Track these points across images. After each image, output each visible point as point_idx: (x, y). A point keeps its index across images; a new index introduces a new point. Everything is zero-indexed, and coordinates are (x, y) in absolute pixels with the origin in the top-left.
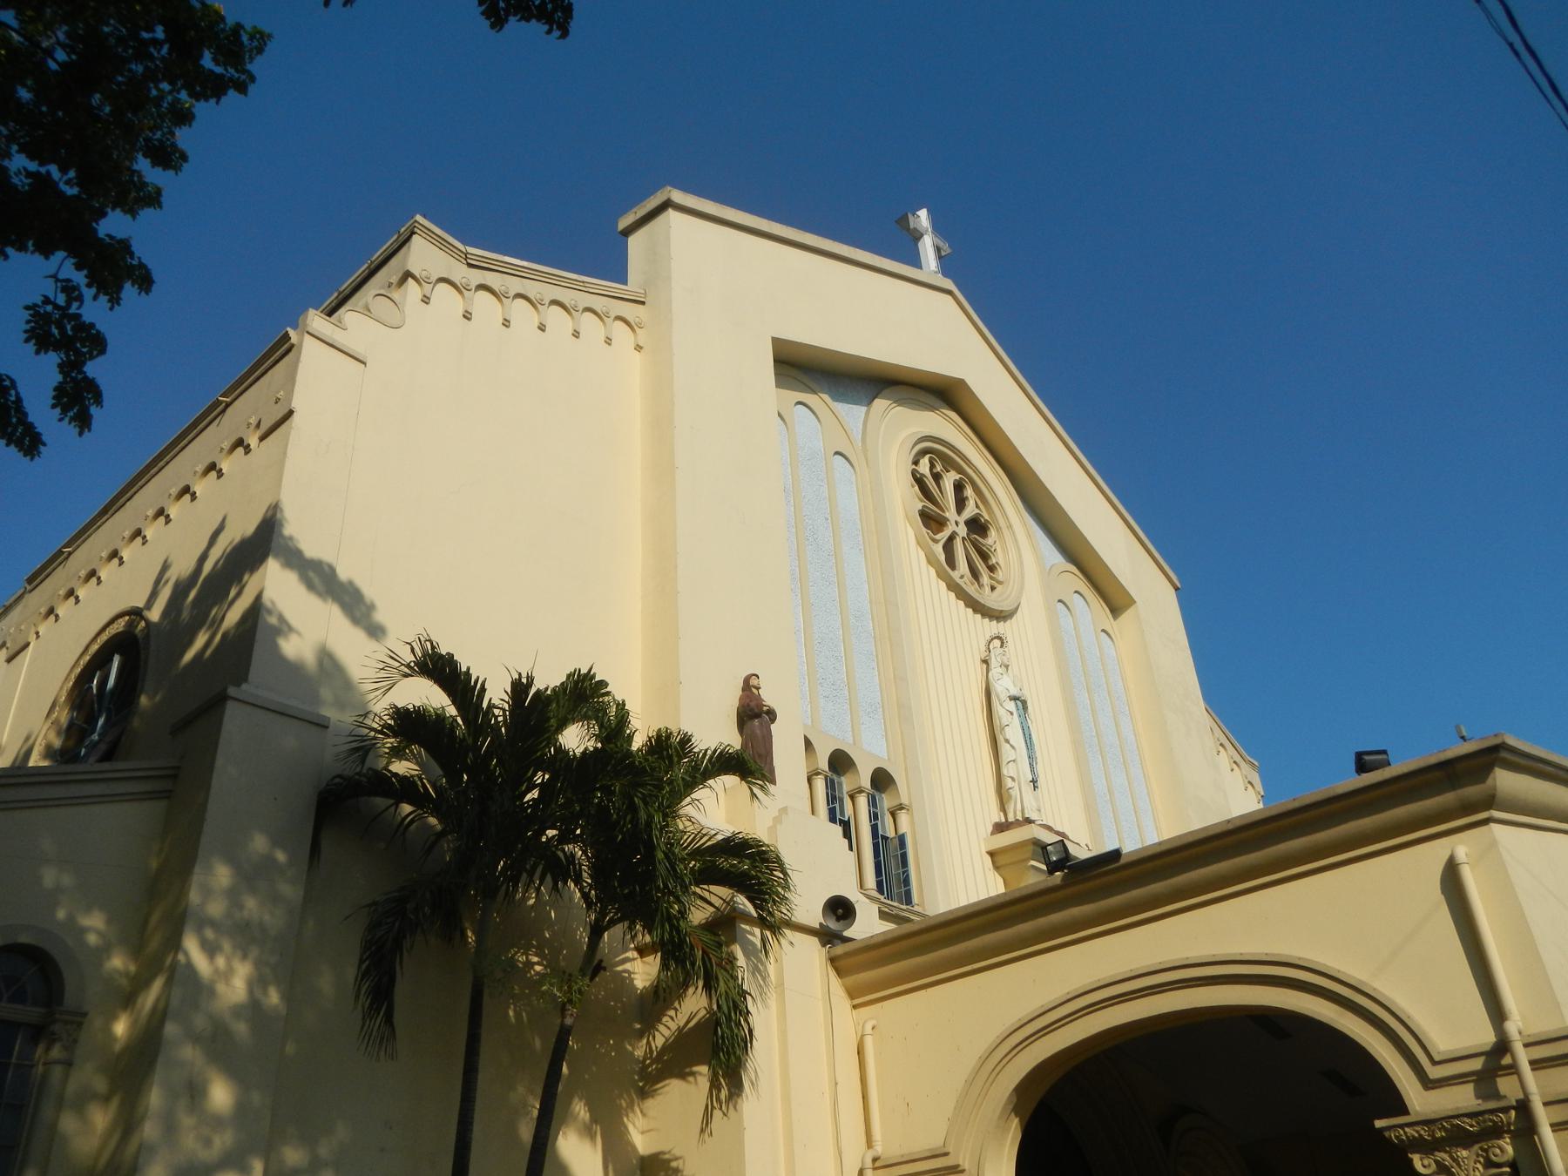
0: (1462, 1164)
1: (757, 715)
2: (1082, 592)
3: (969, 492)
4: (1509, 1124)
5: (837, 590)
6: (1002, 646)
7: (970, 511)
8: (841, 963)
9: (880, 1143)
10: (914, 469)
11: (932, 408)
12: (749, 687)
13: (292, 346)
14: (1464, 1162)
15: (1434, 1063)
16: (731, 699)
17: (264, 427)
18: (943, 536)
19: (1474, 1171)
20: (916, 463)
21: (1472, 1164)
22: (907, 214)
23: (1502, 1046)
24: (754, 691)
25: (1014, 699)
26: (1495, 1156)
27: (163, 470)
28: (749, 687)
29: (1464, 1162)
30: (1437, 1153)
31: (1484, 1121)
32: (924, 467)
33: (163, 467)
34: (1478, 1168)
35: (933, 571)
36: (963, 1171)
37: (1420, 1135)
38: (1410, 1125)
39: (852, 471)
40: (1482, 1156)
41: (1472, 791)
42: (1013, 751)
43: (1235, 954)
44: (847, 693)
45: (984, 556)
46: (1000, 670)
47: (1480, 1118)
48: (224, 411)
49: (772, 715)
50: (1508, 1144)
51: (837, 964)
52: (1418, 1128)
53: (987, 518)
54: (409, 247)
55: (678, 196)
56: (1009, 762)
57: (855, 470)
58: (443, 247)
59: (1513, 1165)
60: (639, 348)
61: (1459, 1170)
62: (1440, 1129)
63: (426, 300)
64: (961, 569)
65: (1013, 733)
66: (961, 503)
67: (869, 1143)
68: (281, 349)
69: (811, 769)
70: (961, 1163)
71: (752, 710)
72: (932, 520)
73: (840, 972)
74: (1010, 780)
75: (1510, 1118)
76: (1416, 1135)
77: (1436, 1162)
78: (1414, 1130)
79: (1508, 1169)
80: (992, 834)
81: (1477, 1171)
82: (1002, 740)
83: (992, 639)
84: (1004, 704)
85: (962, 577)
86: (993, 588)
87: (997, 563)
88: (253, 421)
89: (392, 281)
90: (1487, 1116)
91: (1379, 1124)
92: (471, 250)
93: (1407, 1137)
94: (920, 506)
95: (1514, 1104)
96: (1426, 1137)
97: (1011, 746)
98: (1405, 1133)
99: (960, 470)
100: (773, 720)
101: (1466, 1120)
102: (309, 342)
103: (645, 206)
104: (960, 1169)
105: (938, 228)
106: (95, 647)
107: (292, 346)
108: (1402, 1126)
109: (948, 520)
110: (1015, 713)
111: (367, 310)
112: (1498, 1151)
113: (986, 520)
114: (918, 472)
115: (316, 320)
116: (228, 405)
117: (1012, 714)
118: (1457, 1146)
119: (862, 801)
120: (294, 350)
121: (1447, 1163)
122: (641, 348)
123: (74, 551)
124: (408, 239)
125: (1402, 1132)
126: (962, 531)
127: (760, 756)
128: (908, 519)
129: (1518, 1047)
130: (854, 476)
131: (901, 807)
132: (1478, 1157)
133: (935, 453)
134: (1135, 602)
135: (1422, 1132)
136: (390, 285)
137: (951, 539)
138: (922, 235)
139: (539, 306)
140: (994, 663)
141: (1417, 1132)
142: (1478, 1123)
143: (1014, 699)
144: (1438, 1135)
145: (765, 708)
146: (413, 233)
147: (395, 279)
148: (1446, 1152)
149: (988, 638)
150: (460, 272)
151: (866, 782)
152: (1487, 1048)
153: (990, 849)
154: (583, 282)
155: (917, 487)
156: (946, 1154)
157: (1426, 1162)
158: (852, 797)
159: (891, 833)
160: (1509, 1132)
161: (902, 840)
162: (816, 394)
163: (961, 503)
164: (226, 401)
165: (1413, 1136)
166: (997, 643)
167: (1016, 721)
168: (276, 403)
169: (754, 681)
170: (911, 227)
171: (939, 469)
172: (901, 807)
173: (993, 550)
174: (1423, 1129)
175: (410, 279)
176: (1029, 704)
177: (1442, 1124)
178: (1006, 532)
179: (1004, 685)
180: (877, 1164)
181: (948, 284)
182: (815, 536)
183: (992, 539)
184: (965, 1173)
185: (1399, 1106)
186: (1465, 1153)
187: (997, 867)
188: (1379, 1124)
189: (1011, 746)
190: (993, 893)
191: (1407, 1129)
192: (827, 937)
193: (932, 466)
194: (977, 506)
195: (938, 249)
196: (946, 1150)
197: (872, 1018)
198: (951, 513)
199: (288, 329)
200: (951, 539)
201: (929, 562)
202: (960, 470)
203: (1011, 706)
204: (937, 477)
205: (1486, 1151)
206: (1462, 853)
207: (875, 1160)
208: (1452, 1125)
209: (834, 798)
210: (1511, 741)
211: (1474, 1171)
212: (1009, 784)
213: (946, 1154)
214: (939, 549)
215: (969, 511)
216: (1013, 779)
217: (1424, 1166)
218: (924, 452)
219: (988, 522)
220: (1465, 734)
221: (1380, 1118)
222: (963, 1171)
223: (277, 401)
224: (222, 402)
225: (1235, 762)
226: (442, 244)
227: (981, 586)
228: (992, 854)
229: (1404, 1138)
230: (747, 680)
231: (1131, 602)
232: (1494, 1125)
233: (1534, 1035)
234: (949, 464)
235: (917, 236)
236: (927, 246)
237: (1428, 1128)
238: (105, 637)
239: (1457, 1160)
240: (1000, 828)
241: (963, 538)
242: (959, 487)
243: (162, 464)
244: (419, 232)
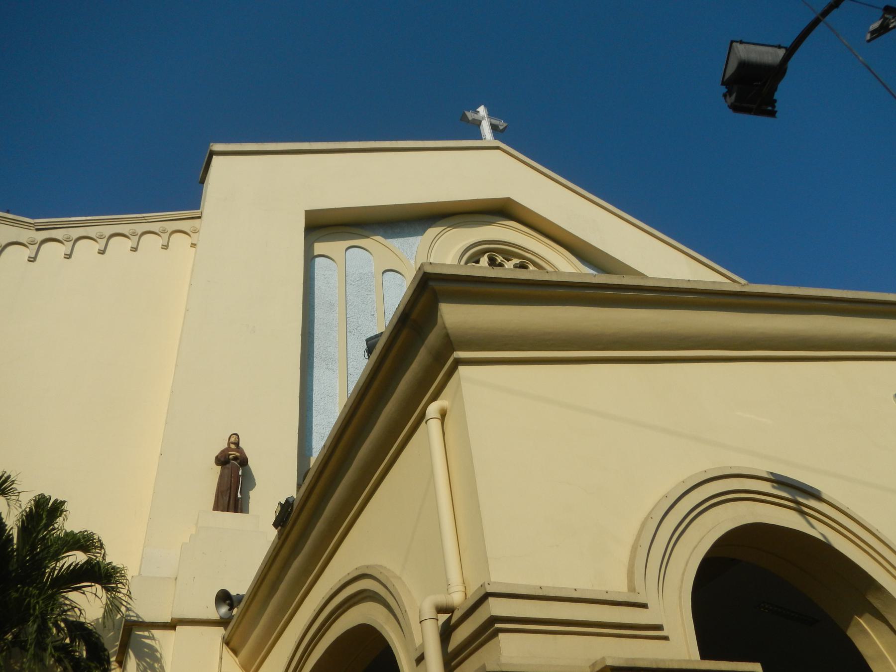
11: (490, 223)
22: (464, 113)
41: (433, 338)
51: (231, 644)
58: (15, 225)
60: (193, 245)
105: (491, 114)
122: (195, 245)
138: (481, 122)
139: (98, 240)
150: (25, 235)
154: (144, 217)
162: (369, 238)
170: (470, 119)
171: (499, 261)
182: (358, 328)
226: (14, 223)
234: (508, 255)
235: (478, 124)
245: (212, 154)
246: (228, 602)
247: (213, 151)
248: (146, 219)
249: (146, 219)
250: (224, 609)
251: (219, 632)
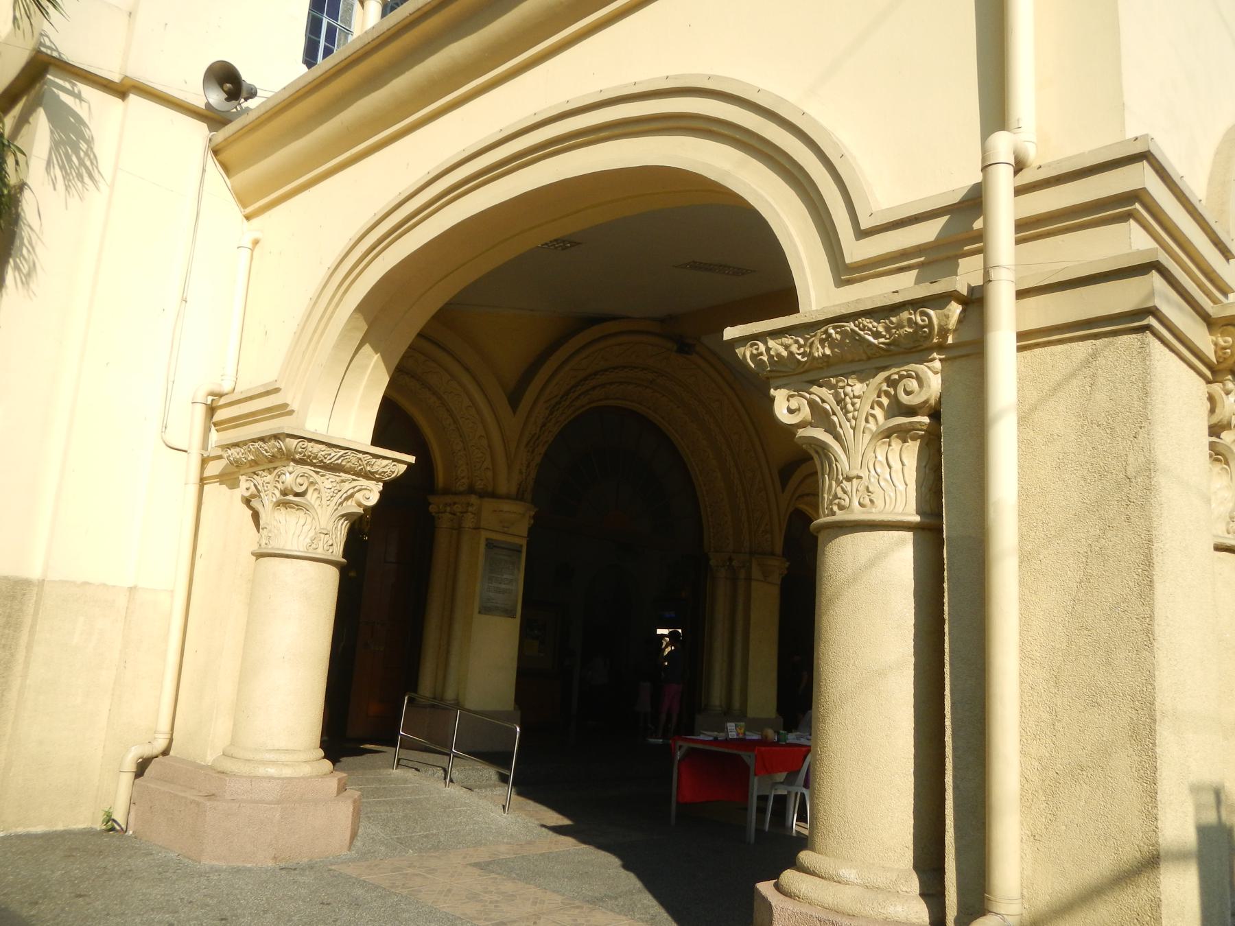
0: (850, 407)
4: (944, 332)
8: (228, 155)
14: (853, 404)
15: (862, 234)
19: (867, 421)
21: (867, 408)
26: (908, 393)
30: (815, 389)
31: (899, 326)
34: (874, 416)
36: (292, 412)
37: (791, 354)
40: (887, 394)
43: (626, 86)
47: (894, 319)
50: (936, 373)
51: (223, 156)
52: (788, 340)
59: (935, 415)
61: (843, 419)
62: (822, 342)
73: (227, 169)
75: (947, 317)
76: (785, 353)
77: (812, 404)
78: (782, 345)
79: (926, 420)
81: (871, 419)
90: (905, 315)
91: (730, 333)
93: (770, 357)
95: (964, 292)
96: (799, 357)
98: (768, 349)
101: (866, 322)
108: (761, 337)
112: (913, 384)
118: (846, 375)
121: (828, 407)
132: (879, 396)
135: (794, 348)
141: (787, 347)
142: (888, 329)
144: (819, 351)
148: (830, 387)
152: (956, 199)
156: (277, 390)
157: (794, 404)
160: (941, 348)
165: (779, 355)
174: (797, 342)
177: (826, 332)
184: (294, 414)
186: (858, 388)
191: (771, 343)
192: (213, 119)
196: (277, 386)
205: (892, 383)
208: (844, 334)
211: (867, 421)
213: (277, 390)
222: (292, 412)
229: (765, 358)
232: (915, 332)
233: (1049, 165)
237: (806, 340)
239: (844, 400)
246: (229, 85)
250: (216, 98)
251: (200, 130)
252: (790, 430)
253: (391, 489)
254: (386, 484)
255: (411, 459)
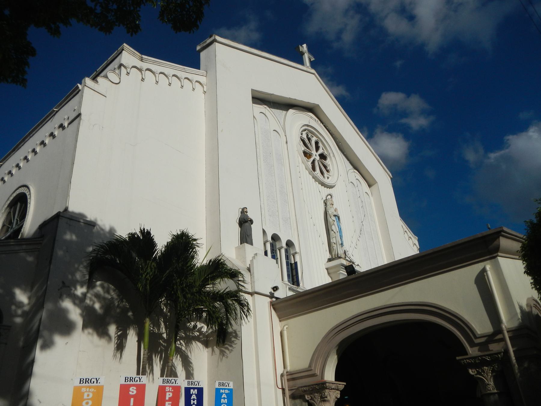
1: (246, 222)
2: (359, 179)
3: (320, 145)
5: (274, 178)
6: (331, 198)
7: (320, 151)
9: (289, 366)
10: (301, 136)
12: (244, 211)
13: (80, 90)
16: (237, 216)
17: (70, 119)
18: (312, 159)
19: (489, 373)
20: (302, 134)
23: (500, 331)
24: (246, 213)
25: (335, 216)
27: (34, 135)
28: (244, 211)
29: (486, 370)
32: (304, 136)
33: (34, 134)
35: (307, 172)
37: (472, 362)
38: (468, 359)
39: (280, 137)
42: (335, 234)
44: (277, 213)
45: (325, 167)
46: (330, 206)
48: (55, 115)
49: (251, 222)
51: (275, 306)
53: (326, 153)
54: (122, 55)
55: (218, 38)
56: (333, 238)
57: (280, 136)
63: (128, 74)
64: (317, 171)
65: (335, 228)
66: (317, 148)
67: (285, 367)
68: (77, 91)
69: (266, 240)
70: (316, 373)
71: (245, 220)
72: (307, 155)
74: (334, 244)
76: (470, 362)
80: (327, 262)
82: (331, 230)
83: (328, 195)
84: (332, 218)
85: (317, 174)
86: (328, 178)
87: (329, 169)
88: (66, 117)
89: (115, 67)
91: (458, 358)
92: (144, 56)
94: (303, 150)
97: (334, 232)
98: (466, 361)
99: (317, 137)
100: (252, 223)
102: (86, 90)
103: (206, 42)
104: (315, 375)
105: (310, 51)
106: (12, 198)
107: (80, 90)
108: (466, 359)
109: (313, 154)
110: (335, 221)
111: (106, 77)
113: (326, 154)
114: (302, 137)
115: (88, 81)
116: (57, 112)
117: (334, 221)
119: (283, 251)
120: (80, 93)
123: (3, 164)
124: (121, 52)
125: (465, 361)
126: (318, 158)
127: (248, 236)
128: (299, 154)
129: (505, 332)
130: (280, 138)
131: (296, 253)
133: (308, 131)
134: (377, 182)
136: (115, 69)
137: (314, 161)
138: (305, 54)
140: (328, 203)
141: (470, 361)
143: (335, 216)
144: (477, 362)
145: (249, 219)
146: (123, 50)
147: (116, 67)
149: (326, 195)
150: (139, 64)
151: (284, 245)
153: (326, 267)
154: (184, 68)
155: (302, 142)
158: (279, 250)
159: (293, 262)
161: (296, 263)
163: (317, 148)
164: (56, 111)
165: (469, 362)
166: (329, 197)
167: (335, 223)
168: (74, 111)
169: (245, 210)
170: (301, 50)
172: (296, 253)
173: (328, 164)
175: (122, 66)
176: (340, 218)
178: (333, 158)
179: (331, 211)
180: (288, 374)
181: (313, 71)
183: (328, 162)
185: (465, 353)
186: (486, 368)
187: (329, 274)
188: (458, 358)
189: (334, 232)
190: (327, 282)
191: (467, 360)
193: (307, 135)
194: (323, 149)
195: (310, 59)
197: (286, 325)
198: (314, 152)
199: (78, 84)
200: (314, 161)
201: (306, 169)
202: (317, 137)
203: (334, 218)
204: (309, 139)
206: (488, 267)
207: (287, 372)
209: (273, 250)
210: (505, 229)
212: (334, 245)
213: (311, 370)
214: (310, 163)
215: (320, 151)
216: (335, 243)
217: (472, 372)
218: (305, 130)
219: (326, 155)
220: (490, 227)
221: (458, 356)
223: (74, 110)
224: (55, 111)
225: (410, 237)
227: (324, 177)
228: (327, 269)
230: (243, 209)
231: (376, 182)
235: (302, 54)
236: (306, 57)
238: (15, 195)
240: (330, 260)
241: (318, 160)
242: (317, 143)
243: (34, 133)
244: (125, 49)
245: (215, 41)
247: (216, 40)
248: (185, 70)
249: (185, 70)
252: (473, 375)
253: (342, 392)
254: (341, 391)
255: (345, 384)
